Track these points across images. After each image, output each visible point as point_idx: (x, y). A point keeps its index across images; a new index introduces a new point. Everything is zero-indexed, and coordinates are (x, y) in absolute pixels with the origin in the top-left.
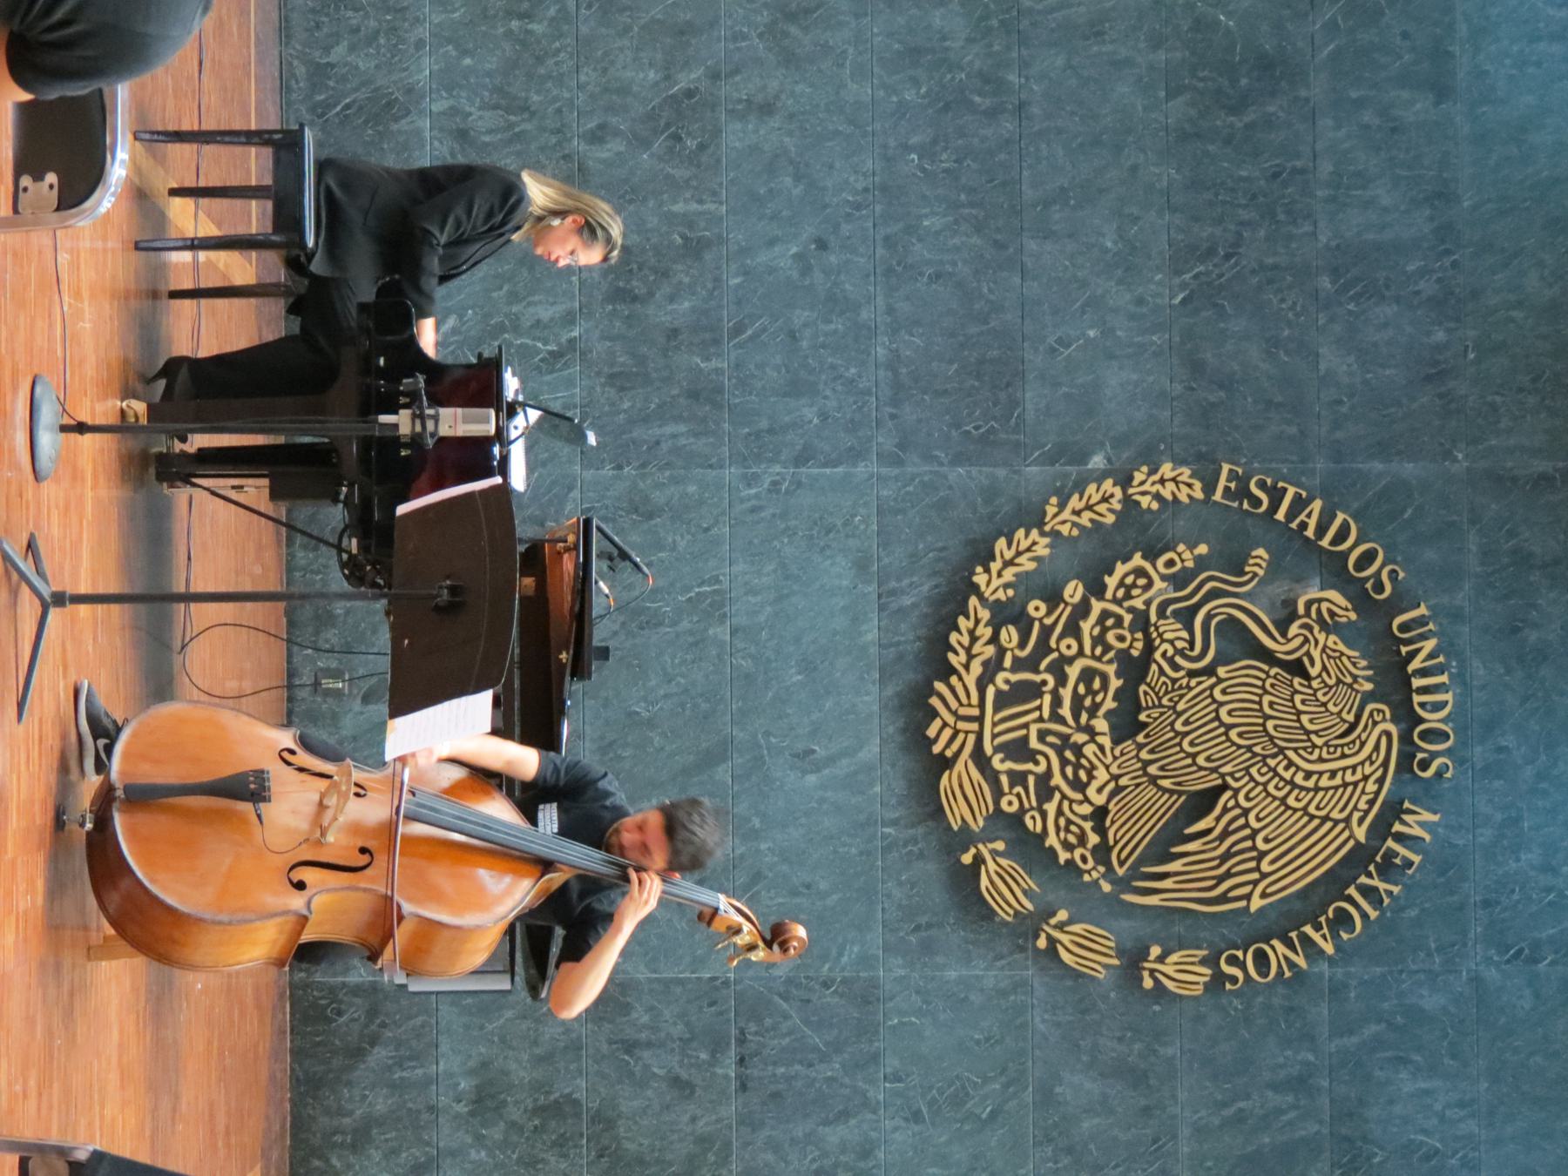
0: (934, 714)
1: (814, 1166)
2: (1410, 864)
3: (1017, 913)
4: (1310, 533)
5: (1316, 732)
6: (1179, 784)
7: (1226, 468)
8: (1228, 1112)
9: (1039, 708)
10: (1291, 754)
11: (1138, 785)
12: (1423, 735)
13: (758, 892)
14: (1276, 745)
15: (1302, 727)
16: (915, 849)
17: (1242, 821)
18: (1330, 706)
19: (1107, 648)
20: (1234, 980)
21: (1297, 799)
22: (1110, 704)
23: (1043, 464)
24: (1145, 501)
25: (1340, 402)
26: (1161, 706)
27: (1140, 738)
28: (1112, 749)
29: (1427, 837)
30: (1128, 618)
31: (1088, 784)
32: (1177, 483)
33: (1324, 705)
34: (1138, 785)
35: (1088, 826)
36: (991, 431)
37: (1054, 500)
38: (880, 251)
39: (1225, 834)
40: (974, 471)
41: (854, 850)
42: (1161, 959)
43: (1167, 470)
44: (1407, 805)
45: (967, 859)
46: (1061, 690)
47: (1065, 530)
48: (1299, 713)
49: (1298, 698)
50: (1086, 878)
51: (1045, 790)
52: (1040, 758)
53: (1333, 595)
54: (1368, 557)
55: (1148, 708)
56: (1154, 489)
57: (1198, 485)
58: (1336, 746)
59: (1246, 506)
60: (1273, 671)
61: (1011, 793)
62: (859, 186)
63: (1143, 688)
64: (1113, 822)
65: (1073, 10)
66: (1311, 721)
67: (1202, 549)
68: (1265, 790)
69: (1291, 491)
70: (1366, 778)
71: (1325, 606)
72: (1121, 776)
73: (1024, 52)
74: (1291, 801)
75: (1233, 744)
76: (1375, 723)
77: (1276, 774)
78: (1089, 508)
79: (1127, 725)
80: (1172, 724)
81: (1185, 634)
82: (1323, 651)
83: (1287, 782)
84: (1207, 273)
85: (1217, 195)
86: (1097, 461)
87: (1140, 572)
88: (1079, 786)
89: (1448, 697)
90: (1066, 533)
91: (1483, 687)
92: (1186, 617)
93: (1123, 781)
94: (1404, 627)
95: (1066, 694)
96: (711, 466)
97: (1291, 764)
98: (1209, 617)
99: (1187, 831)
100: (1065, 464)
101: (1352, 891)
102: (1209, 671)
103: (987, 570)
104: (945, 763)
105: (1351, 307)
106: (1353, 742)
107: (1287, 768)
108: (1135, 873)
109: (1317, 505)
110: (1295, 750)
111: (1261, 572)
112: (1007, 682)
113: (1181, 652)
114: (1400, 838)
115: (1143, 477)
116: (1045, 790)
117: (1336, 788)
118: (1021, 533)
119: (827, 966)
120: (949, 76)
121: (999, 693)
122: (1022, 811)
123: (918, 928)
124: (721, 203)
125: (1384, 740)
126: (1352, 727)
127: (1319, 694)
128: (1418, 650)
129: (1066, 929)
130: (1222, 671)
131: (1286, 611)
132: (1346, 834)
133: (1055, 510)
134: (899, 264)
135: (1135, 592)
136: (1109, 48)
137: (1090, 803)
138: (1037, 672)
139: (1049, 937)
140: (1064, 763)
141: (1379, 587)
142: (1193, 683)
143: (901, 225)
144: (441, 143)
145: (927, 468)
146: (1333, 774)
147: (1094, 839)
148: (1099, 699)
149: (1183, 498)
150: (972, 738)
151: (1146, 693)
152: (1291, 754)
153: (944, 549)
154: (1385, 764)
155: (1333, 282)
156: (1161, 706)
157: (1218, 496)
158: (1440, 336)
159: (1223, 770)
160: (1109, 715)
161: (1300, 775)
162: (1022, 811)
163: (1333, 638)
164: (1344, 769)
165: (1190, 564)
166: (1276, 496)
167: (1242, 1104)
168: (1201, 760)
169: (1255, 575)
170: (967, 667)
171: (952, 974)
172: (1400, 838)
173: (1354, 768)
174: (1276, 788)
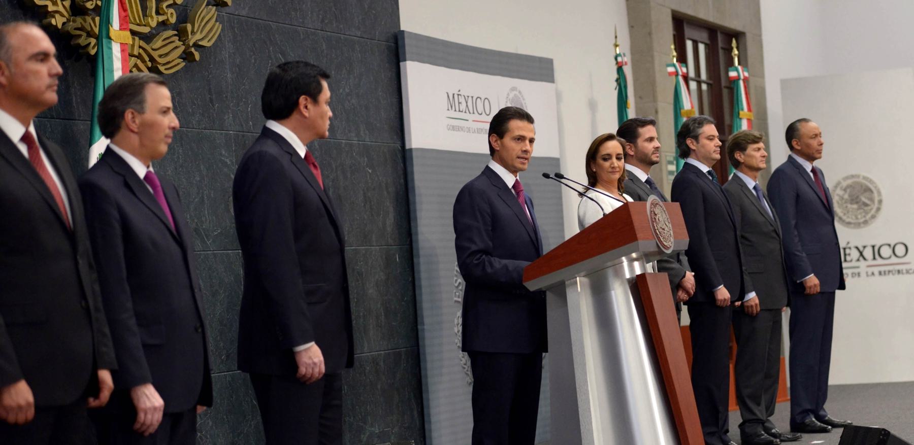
13: (203, 229)
45: (197, 56)
103: (52, 14)
123: (211, 100)
150: (142, 43)
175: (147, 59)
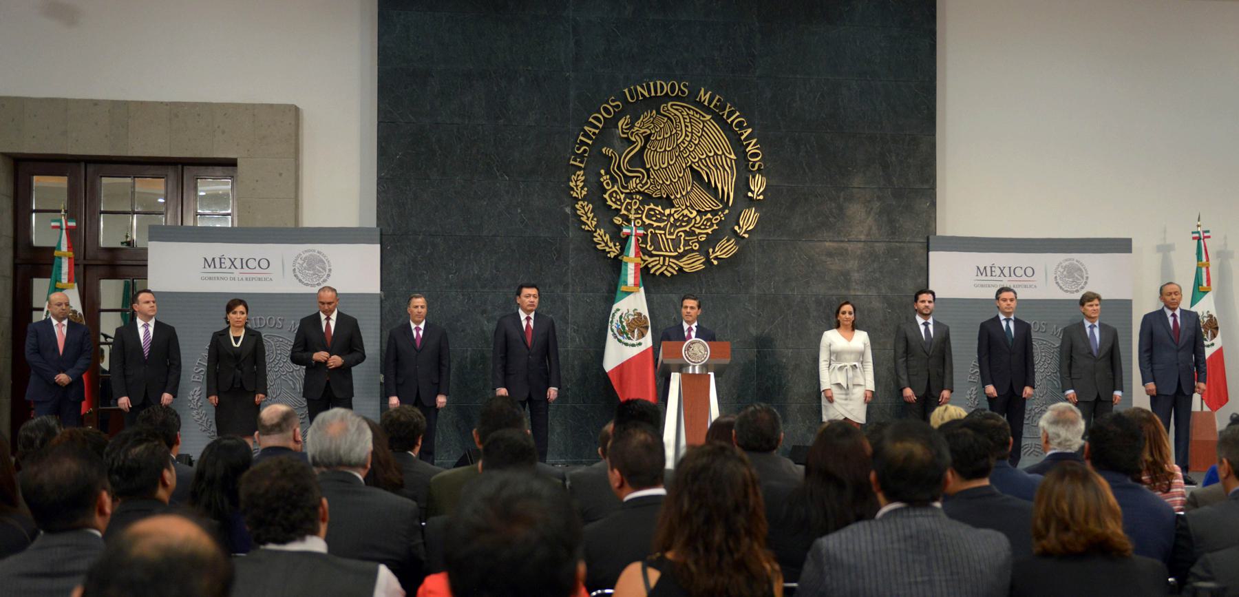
0: (662, 274)
1: (824, 321)
2: (719, 100)
3: (734, 245)
4: (597, 131)
5: (671, 132)
6: (689, 183)
7: (572, 162)
8: (807, 170)
9: (661, 234)
10: (679, 142)
11: (690, 199)
12: (672, 93)
14: (676, 147)
15: (669, 137)
17: (703, 161)
18: (662, 126)
19: (639, 208)
20: (760, 166)
21: (696, 140)
22: (660, 208)
23: (568, 230)
24: (584, 193)
25: (547, 118)
26: (660, 189)
27: (673, 197)
28: (676, 208)
29: (710, 92)
30: (628, 200)
31: (689, 217)
32: (577, 180)
33: (661, 128)
34: (690, 199)
35: (704, 218)
36: (556, 249)
37: (583, 227)
38: (486, 290)
39: (707, 166)
40: (570, 256)
41: (711, 304)
42: (753, 192)
43: (572, 184)
44: (698, 99)
45: (715, 262)
46: (654, 226)
47: (594, 223)
48: (664, 138)
49: (658, 138)
50: (723, 219)
51: (691, 233)
53: (620, 124)
54: (606, 109)
55: (661, 194)
56: (580, 189)
57: (578, 173)
58: (676, 125)
59: (586, 155)
60: (648, 146)
62: (461, 298)
63: (654, 196)
64: (703, 208)
65: (394, 214)
66: (667, 134)
67: (603, 172)
68: (692, 152)
69: (581, 138)
70: (688, 114)
71: (624, 127)
72: (686, 205)
73: (410, 233)
74: (696, 142)
75: (675, 163)
76: (668, 110)
77: (686, 147)
78: (586, 214)
79: (668, 203)
80: (667, 185)
81: (634, 179)
82: (641, 128)
83: (689, 143)
84: (497, 166)
85: (467, 162)
86: (568, 210)
87: (611, 196)
89: (658, 83)
90: (595, 223)
91: (654, 70)
92: (628, 179)
93: (688, 204)
94: (632, 98)
95: (655, 224)
96: (568, 355)
97: (683, 142)
98: (628, 170)
99: (707, 181)
100: (569, 222)
101: (729, 121)
102: (648, 171)
104: (681, 269)
105: (510, 113)
106: (675, 118)
107: (684, 143)
108: (722, 201)
109: (586, 128)
110: (677, 140)
111: (611, 150)
112: (650, 246)
113: (640, 182)
114: (710, 103)
115: (575, 193)
117: (692, 125)
118: (595, 239)
119: (753, 315)
120: (420, 262)
121: (655, 249)
124: (467, 350)
125: (674, 107)
126: (669, 118)
127: (657, 130)
128: (641, 92)
130: (648, 166)
131: (624, 141)
132: (708, 122)
133: (587, 226)
134: (491, 283)
135: (618, 197)
136: (409, 200)
138: (647, 235)
139: (744, 233)
140: (681, 226)
141: (617, 106)
142: (652, 177)
143: (477, 282)
144: (442, 456)
145: (570, 274)
146: (686, 126)
147: (709, 215)
148: (658, 212)
149: (583, 178)
150: (671, 260)
151: (656, 195)
152: (679, 142)
153: (600, 268)
154: (683, 107)
155: (501, 119)
156: (660, 189)
157: (582, 166)
158: (522, 79)
159: (684, 167)
160: (664, 210)
161: (687, 138)
162: (698, 242)
163: (636, 124)
164: (685, 122)
165: (608, 177)
166: (583, 143)
167: (804, 165)
168: (681, 175)
169: (612, 152)
170: (645, 261)
171: (756, 270)
172: (710, 103)
173: (684, 118)
174: (691, 147)
175: (674, 266)
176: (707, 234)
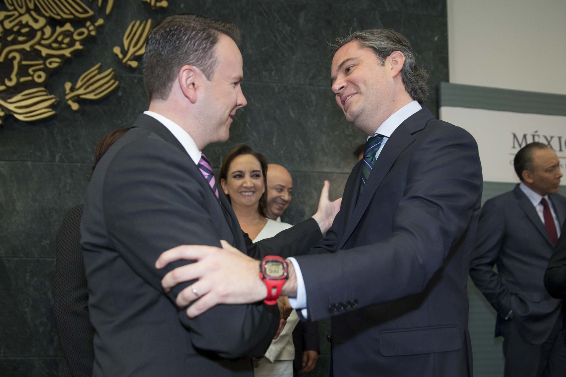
16: (71, 142)
35: (59, 30)
41: (69, 181)
45: (75, 106)
52: (10, 56)
61: (32, 76)
64: (58, 14)
88: (32, 33)
93: (31, 6)
116: (35, 54)
122: (46, 70)
129: (126, 48)
137: (44, 27)
140: (15, 42)
147: (68, 27)
162: (46, 70)
176: (62, 56)
